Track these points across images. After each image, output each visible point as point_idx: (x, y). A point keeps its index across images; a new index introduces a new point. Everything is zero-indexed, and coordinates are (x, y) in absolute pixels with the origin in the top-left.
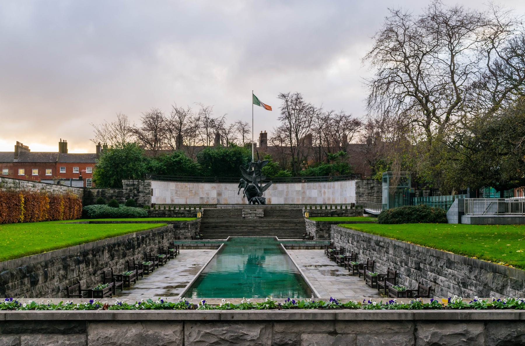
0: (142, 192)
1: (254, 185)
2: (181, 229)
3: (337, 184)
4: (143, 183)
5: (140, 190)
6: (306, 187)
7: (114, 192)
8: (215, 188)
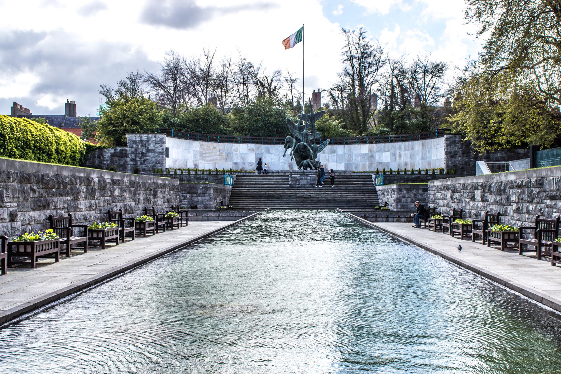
0: (153, 151)
1: (305, 144)
2: (199, 195)
3: (417, 145)
4: (154, 139)
5: (150, 148)
7: (115, 150)
8: (253, 150)
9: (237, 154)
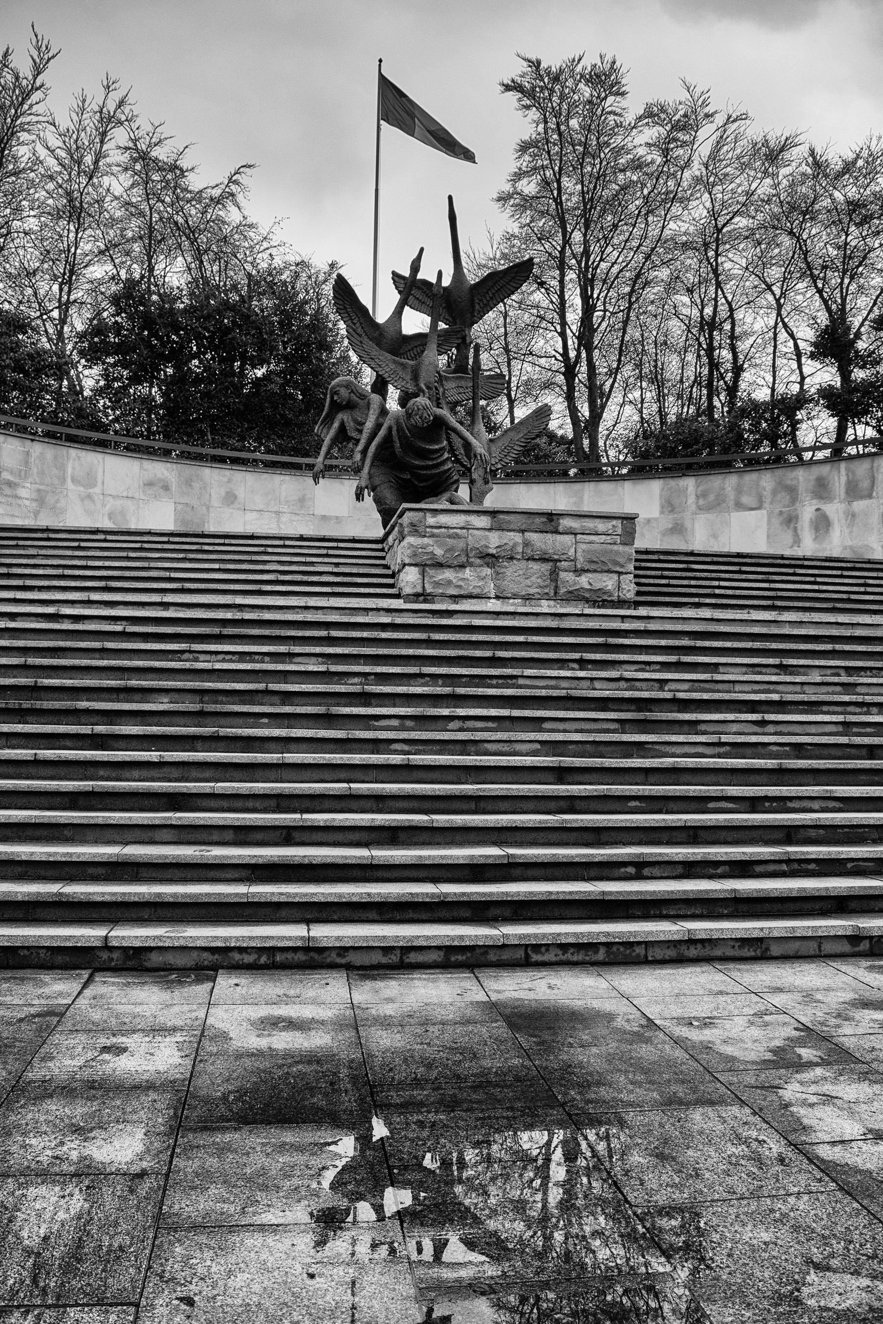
6: (691, 499)
8: (166, 488)
9: (89, 497)
